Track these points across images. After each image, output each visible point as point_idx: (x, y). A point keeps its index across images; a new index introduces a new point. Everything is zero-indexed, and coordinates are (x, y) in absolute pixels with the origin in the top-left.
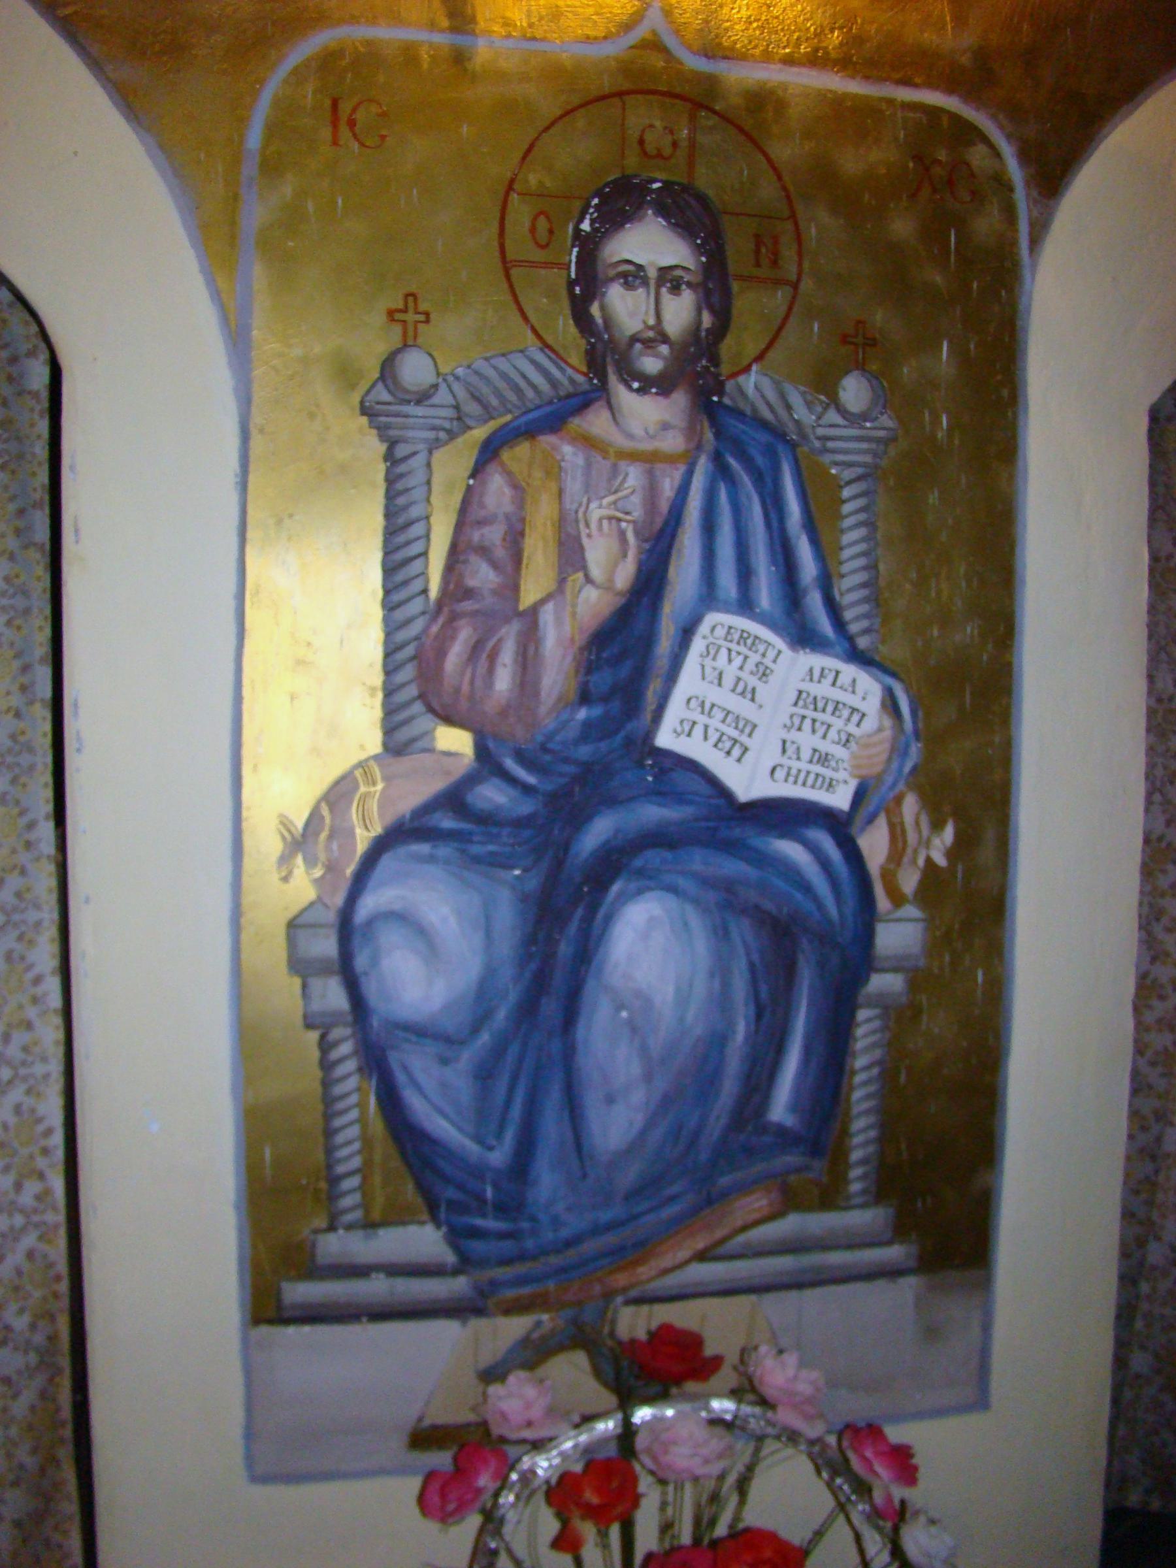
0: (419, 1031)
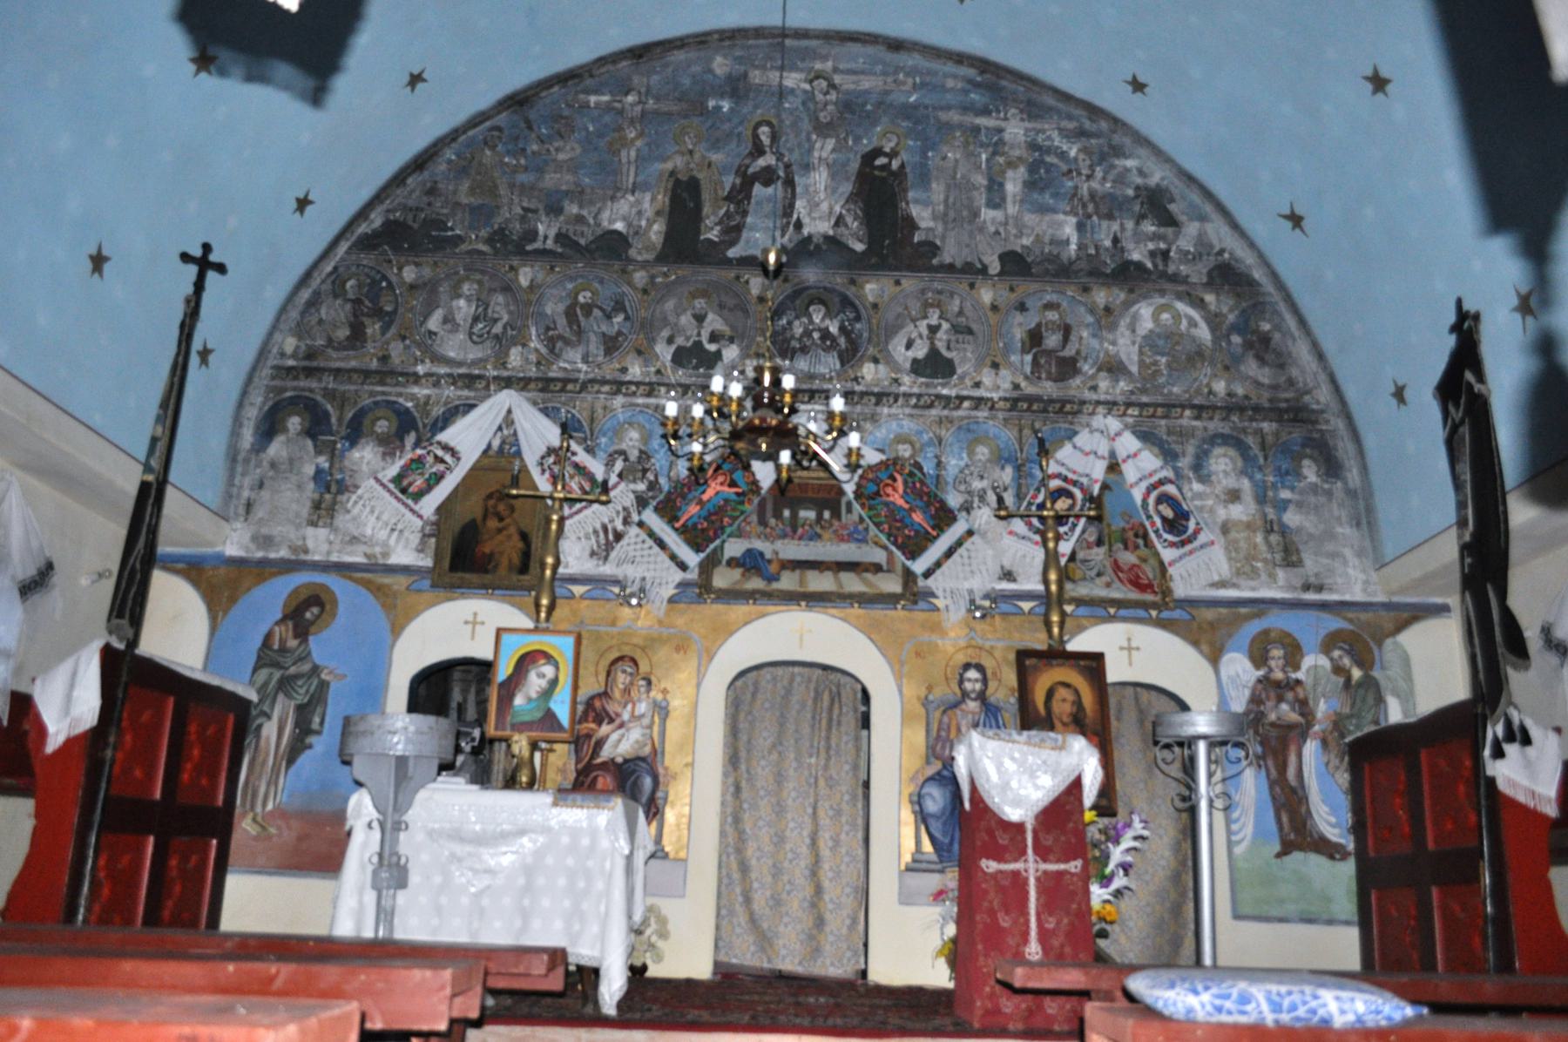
0: (933, 816)
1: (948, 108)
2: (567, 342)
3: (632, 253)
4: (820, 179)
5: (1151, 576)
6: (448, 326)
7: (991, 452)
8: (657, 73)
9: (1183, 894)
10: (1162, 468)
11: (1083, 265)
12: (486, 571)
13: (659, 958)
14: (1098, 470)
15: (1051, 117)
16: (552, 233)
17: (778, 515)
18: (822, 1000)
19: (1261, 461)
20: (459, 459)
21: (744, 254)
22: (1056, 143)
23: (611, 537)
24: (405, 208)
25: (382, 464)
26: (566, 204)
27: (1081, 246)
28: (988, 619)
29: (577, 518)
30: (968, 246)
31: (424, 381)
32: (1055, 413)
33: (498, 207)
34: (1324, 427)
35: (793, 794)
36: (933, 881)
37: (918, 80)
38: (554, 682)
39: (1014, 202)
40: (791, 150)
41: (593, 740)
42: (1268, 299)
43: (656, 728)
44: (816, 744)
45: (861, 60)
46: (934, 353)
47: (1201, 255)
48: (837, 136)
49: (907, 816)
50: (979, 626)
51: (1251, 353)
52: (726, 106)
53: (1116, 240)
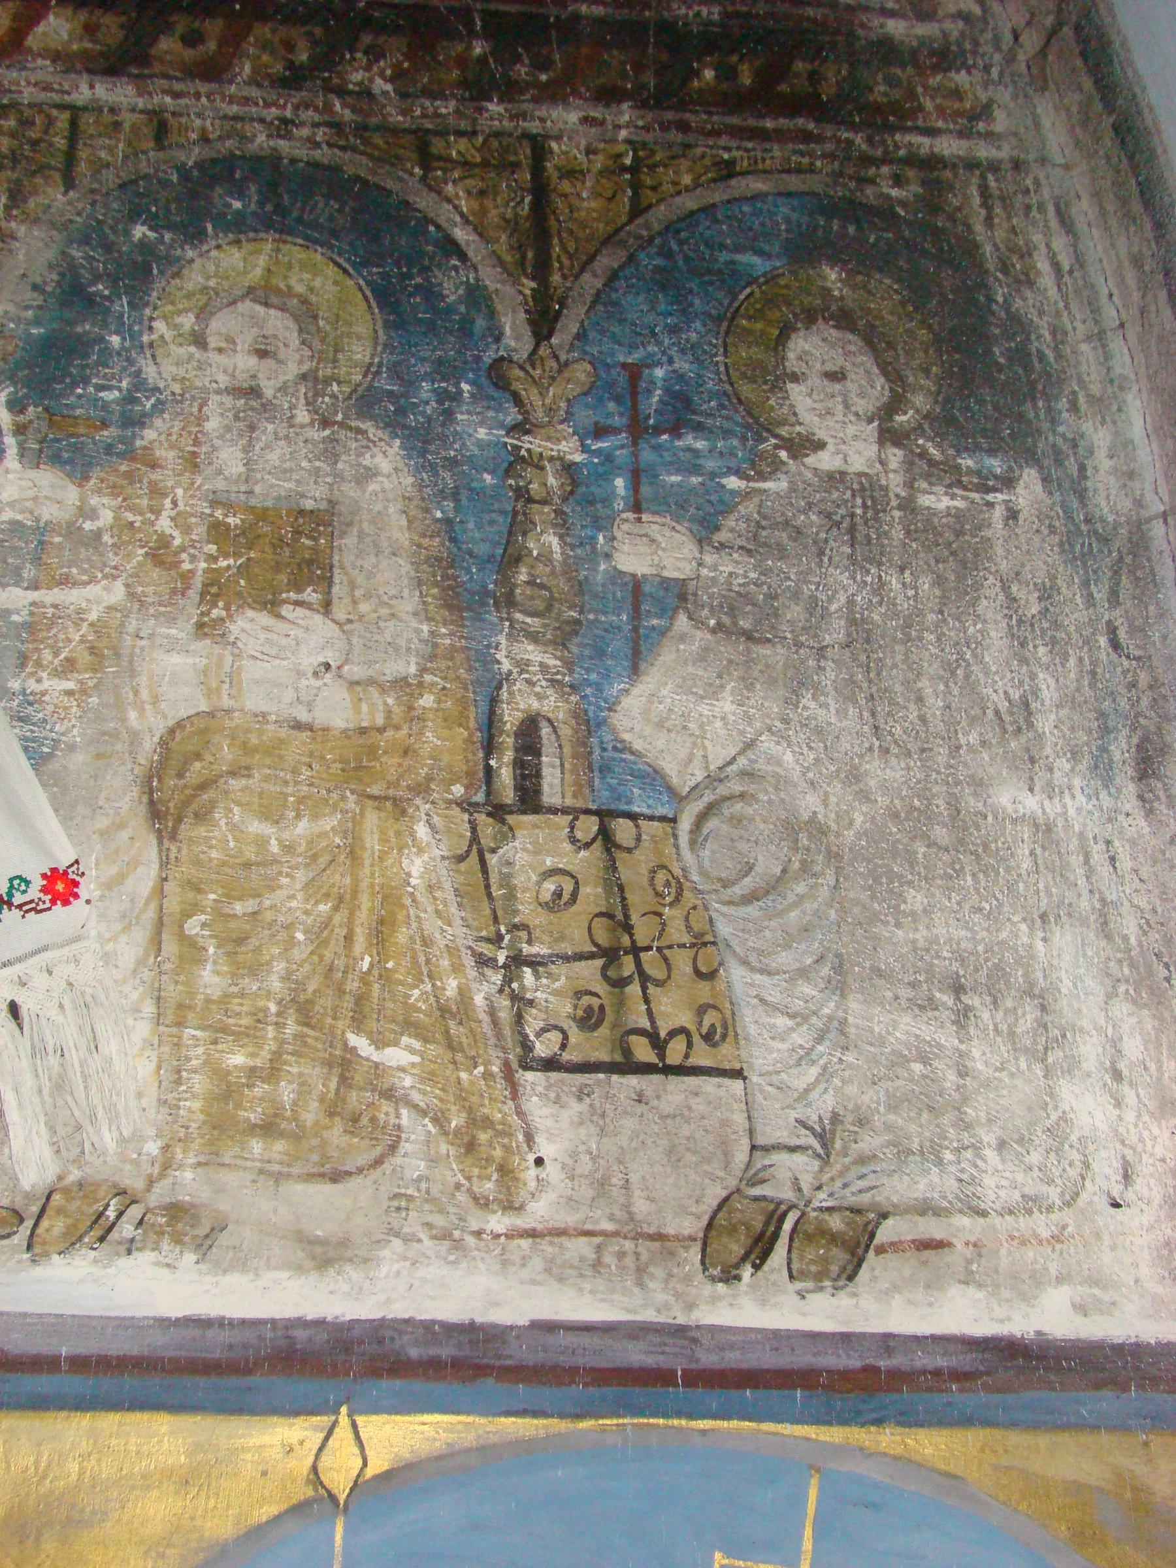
34: (949, 146)
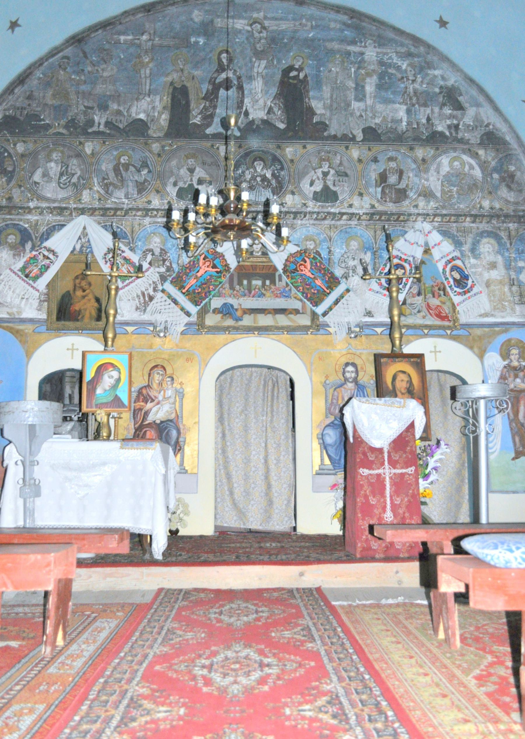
0: (330, 445)
1: (332, 40)
2: (116, 187)
3: (150, 132)
4: (258, 85)
5: (447, 312)
6: (46, 179)
7: (359, 244)
8: (159, 21)
9: (462, 481)
10: (454, 251)
11: (410, 134)
12: (78, 320)
13: (185, 526)
14: (419, 254)
15: (392, 45)
16: (103, 121)
17: (240, 283)
18: (274, 545)
19: (508, 245)
20: (57, 256)
21: (216, 132)
22: (395, 61)
23: (147, 299)
24: (16, 108)
25: (13, 261)
26: (110, 103)
27: (409, 123)
28: (358, 337)
29: (127, 288)
30: (344, 124)
31: (34, 211)
32: (394, 221)
33: (70, 106)
35: (254, 437)
36: (331, 480)
37: (314, 23)
38: (118, 380)
39: (371, 97)
40: (240, 68)
41: (143, 412)
42: (513, 152)
43: (177, 404)
44: (265, 409)
45: (280, 12)
46: (326, 188)
47: (476, 127)
48: (267, 59)
49: (316, 446)
50: (353, 342)
51: (504, 184)
52: (201, 41)
53: (429, 119)
